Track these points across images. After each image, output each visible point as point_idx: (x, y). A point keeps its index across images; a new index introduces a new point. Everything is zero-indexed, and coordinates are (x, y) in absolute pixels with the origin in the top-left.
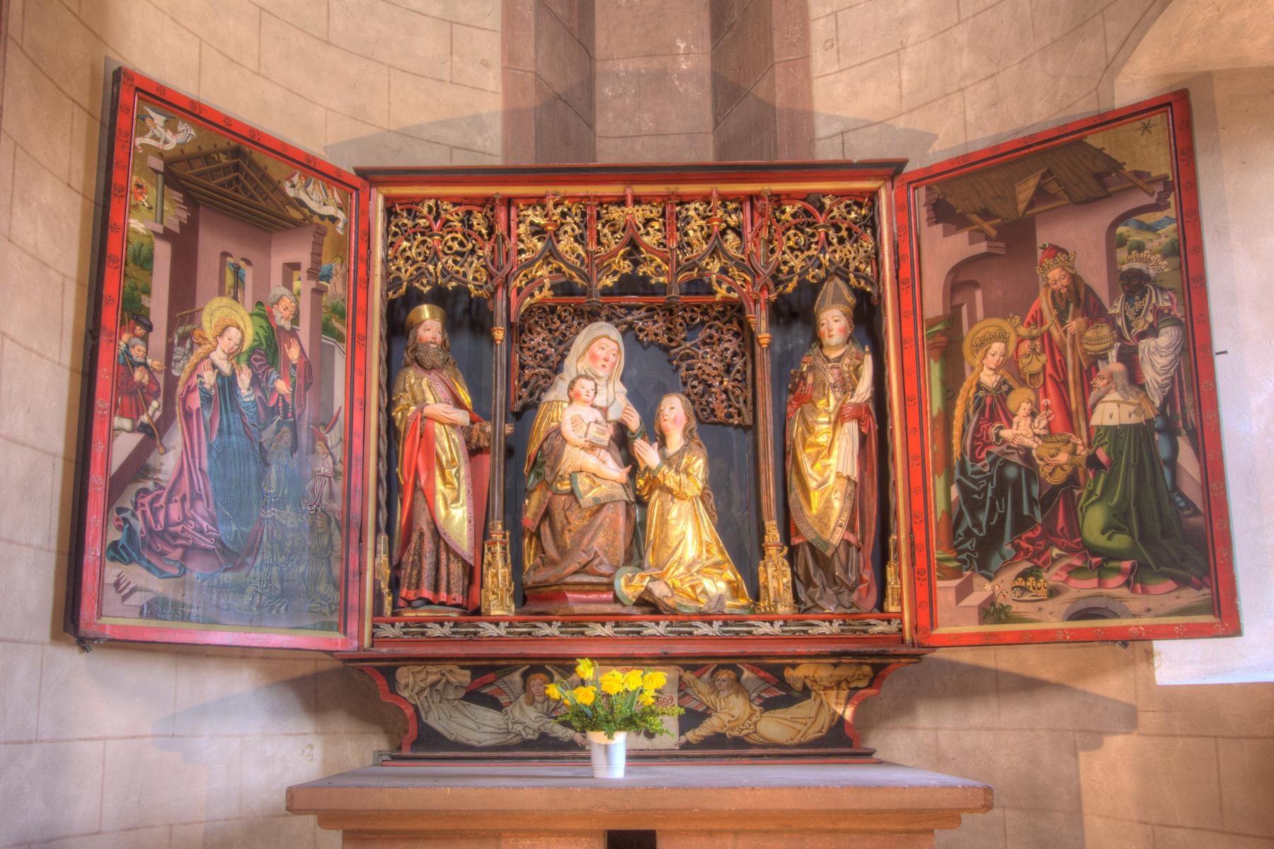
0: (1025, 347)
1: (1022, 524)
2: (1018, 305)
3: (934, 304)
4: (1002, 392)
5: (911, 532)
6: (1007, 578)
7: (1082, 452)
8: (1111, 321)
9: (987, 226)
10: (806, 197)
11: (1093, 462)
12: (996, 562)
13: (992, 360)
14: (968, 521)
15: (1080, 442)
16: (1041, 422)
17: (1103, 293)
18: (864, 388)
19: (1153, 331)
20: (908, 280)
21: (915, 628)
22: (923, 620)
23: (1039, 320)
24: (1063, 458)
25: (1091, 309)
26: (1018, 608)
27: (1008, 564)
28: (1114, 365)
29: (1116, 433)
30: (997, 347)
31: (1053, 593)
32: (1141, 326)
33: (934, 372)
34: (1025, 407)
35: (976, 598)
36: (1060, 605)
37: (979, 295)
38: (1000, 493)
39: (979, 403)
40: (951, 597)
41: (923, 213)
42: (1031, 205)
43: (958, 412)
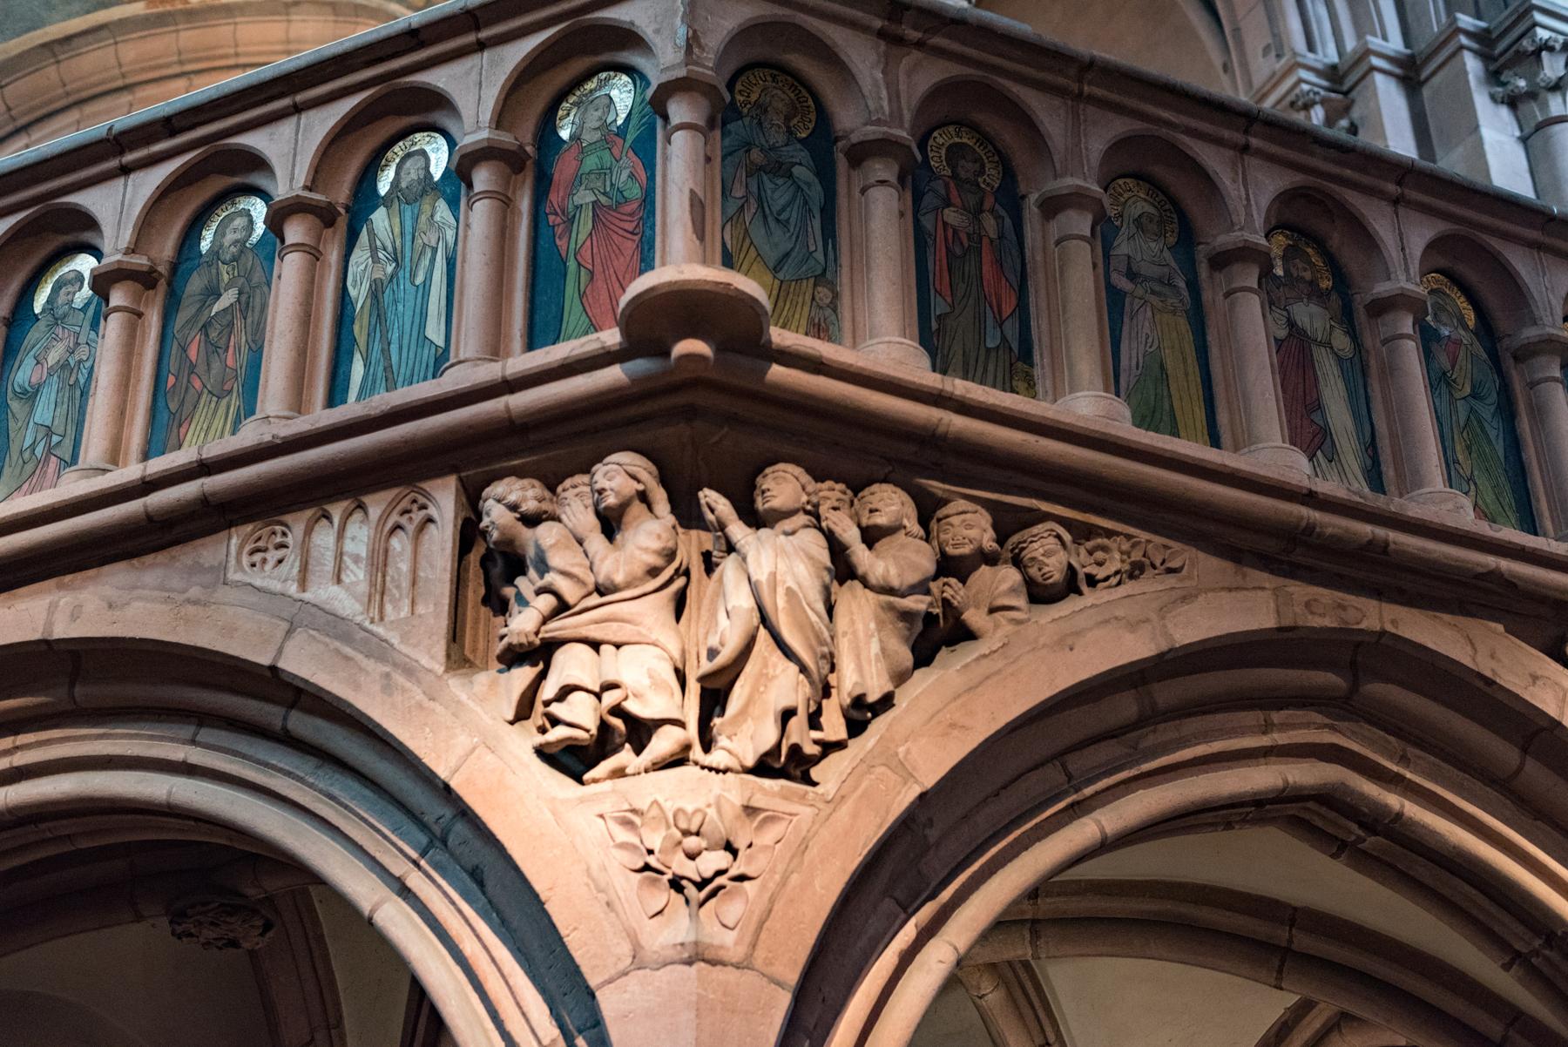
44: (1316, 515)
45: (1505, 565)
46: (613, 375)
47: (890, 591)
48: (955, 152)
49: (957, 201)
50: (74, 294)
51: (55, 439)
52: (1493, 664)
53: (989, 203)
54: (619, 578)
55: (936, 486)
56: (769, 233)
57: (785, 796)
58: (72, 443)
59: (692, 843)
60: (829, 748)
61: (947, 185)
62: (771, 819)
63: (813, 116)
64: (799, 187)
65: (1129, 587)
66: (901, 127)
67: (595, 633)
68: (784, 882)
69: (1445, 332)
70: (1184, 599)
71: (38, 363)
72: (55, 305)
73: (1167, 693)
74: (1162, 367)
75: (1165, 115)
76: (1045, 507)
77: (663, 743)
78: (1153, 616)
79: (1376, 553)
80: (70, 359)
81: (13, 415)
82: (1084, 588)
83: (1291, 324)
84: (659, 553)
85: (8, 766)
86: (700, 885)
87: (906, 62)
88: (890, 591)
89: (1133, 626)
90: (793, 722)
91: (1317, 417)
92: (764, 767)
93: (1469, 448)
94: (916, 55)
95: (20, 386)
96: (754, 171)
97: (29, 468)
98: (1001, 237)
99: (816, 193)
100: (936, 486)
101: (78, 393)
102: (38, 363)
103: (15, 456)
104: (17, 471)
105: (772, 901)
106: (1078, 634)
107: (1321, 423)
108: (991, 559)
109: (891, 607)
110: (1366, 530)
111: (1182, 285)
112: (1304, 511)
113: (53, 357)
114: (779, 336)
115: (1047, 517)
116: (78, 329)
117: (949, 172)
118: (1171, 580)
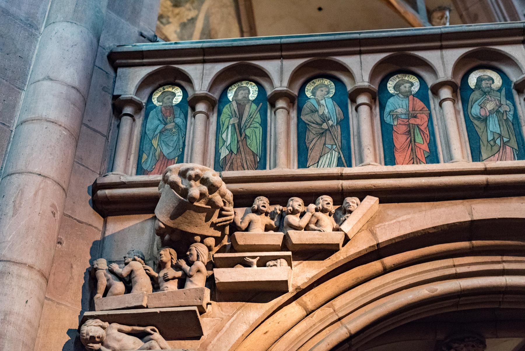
50: (491, 84)
51: (505, 140)
58: (516, 142)
71: (481, 108)
72: (481, 87)
80: (500, 109)
81: (477, 126)
85: (502, 268)
95: (476, 115)
97: (496, 149)
101: (511, 124)
102: (481, 108)
103: (485, 143)
104: (489, 148)
113: (490, 106)
116: (499, 99)
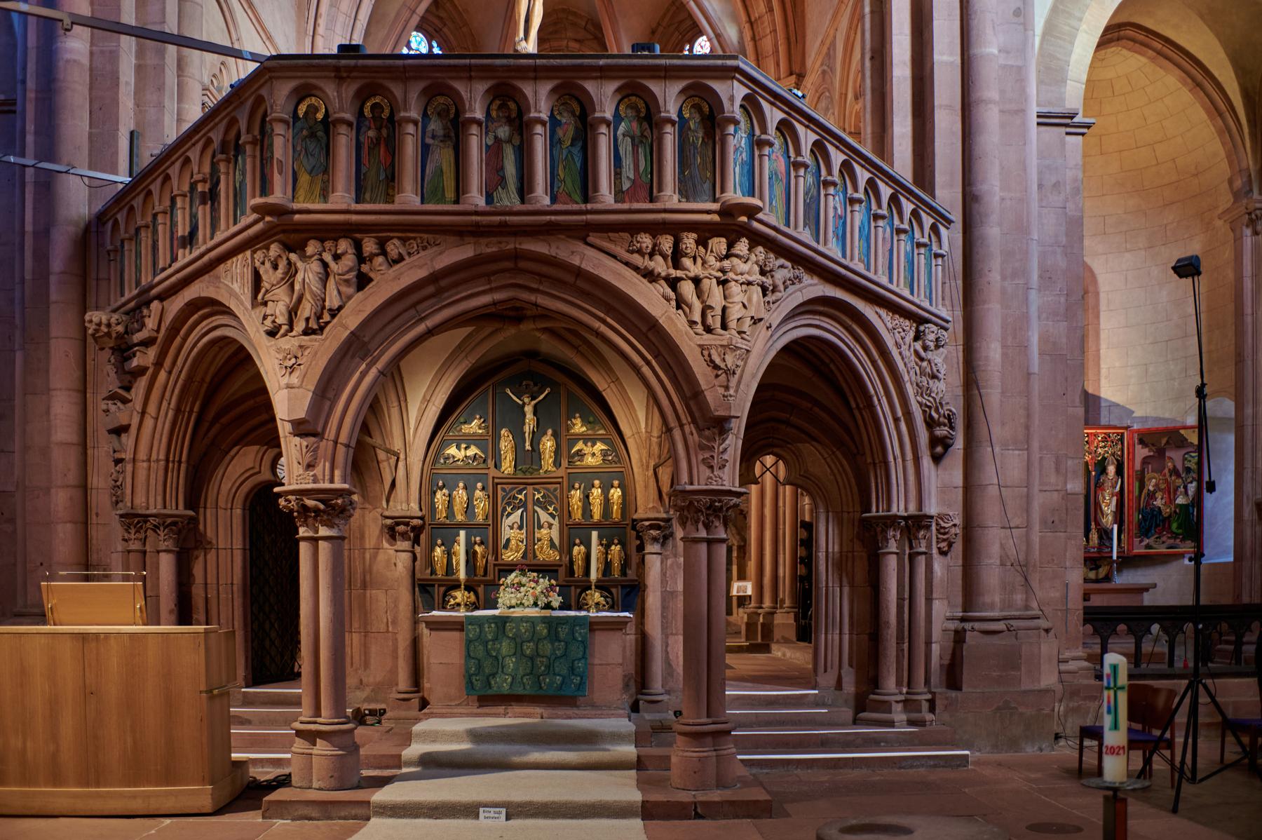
0: (1161, 481)
1: (1157, 526)
2: (1161, 471)
3: (1138, 466)
4: (1154, 492)
5: (1128, 526)
6: (1153, 538)
7: (1173, 509)
8: (1182, 478)
9: (1153, 448)
10: (1105, 433)
11: (1175, 512)
12: (1150, 535)
13: (1152, 484)
14: (1143, 524)
15: (1173, 507)
16: (1164, 501)
17: (1181, 471)
18: (1118, 488)
19: (1191, 482)
20: (1132, 459)
21: (1128, 550)
22: (1131, 548)
23: (1165, 475)
24: (1168, 510)
25: (1178, 476)
26: (1155, 546)
27: (1153, 535)
28: (1182, 489)
29: (1181, 506)
30: (1154, 480)
31: (1163, 542)
32: (1189, 480)
33: (1137, 484)
34: (1160, 497)
35: (1144, 543)
36: (1165, 545)
37: (1150, 466)
38: (1152, 518)
39: (1148, 494)
40: (1137, 543)
41: (1136, 441)
42: (1165, 445)
43: (1143, 496)
44: (478, 218)
45: (553, 218)
46: (259, 226)
47: (339, 275)
48: (374, 107)
49: (373, 126)
52: (558, 251)
53: (384, 124)
54: (275, 283)
55: (358, 236)
56: (308, 160)
57: (311, 341)
59: (289, 356)
60: (327, 323)
61: (370, 122)
62: (308, 347)
63: (324, 110)
64: (319, 140)
65: (422, 253)
66: (343, 111)
67: (272, 298)
68: (310, 365)
69: (564, 120)
70: (440, 254)
73: (443, 283)
74: (442, 171)
75: (438, 75)
76: (392, 235)
77: (282, 331)
78: (429, 262)
79: (503, 225)
82: (407, 257)
83: (496, 137)
84: (283, 273)
86: (290, 368)
87: (344, 87)
88: (339, 275)
89: (420, 267)
90: (311, 321)
91: (501, 173)
92: (306, 332)
93: (565, 168)
94: (349, 80)
96: (304, 139)
98: (388, 135)
99: (324, 141)
100: (358, 236)
105: (307, 370)
106: (401, 274)
107: (501, 173)
108: (377, 255)
109: (341, 279)
110: (498, 218)
111: (453, 134)
112: (474, 218)
114: (296, 206)
115: (392, 238)
117: (371, 116)
118: (435, 248)
